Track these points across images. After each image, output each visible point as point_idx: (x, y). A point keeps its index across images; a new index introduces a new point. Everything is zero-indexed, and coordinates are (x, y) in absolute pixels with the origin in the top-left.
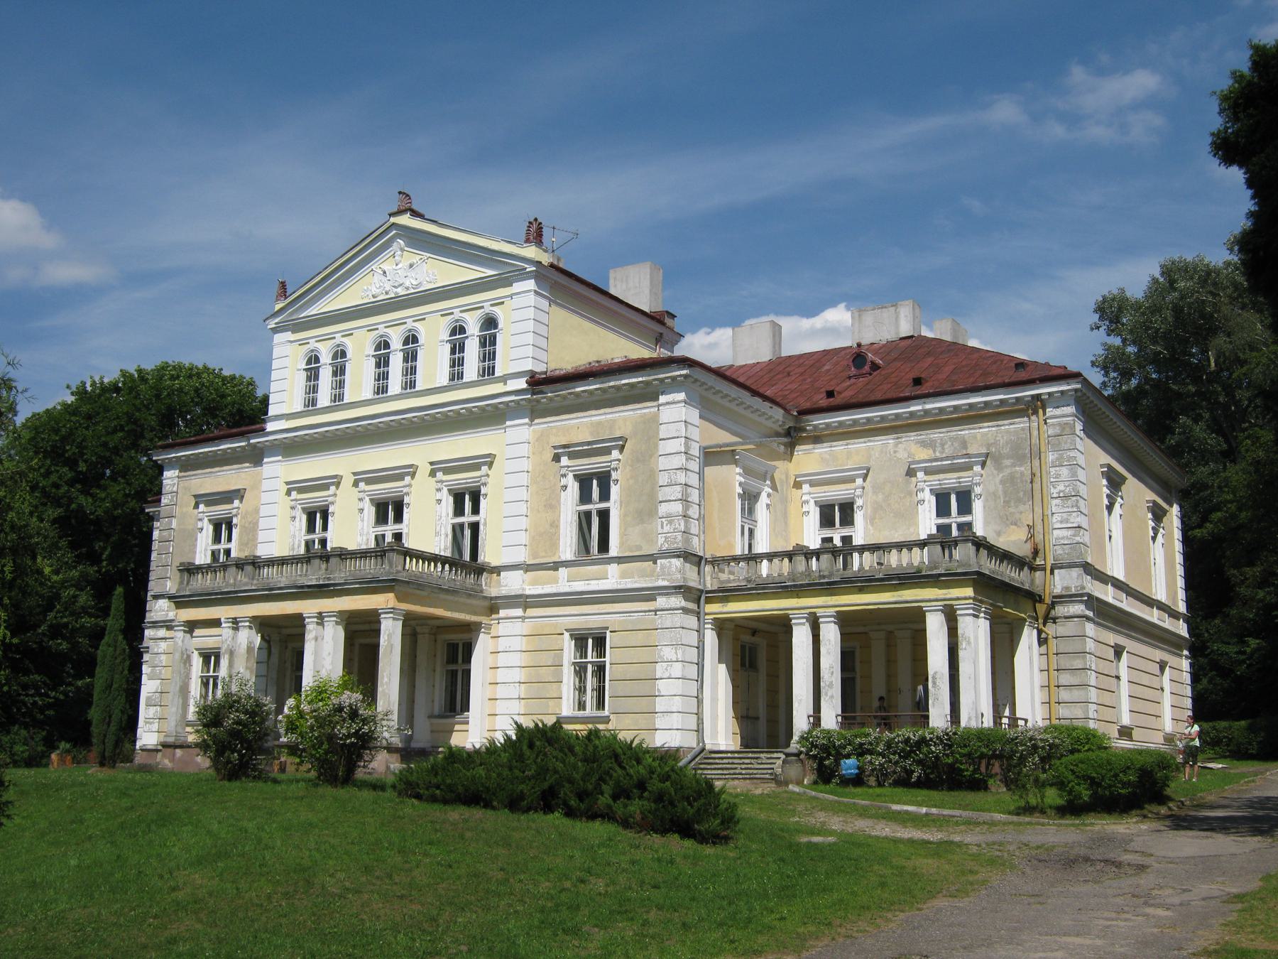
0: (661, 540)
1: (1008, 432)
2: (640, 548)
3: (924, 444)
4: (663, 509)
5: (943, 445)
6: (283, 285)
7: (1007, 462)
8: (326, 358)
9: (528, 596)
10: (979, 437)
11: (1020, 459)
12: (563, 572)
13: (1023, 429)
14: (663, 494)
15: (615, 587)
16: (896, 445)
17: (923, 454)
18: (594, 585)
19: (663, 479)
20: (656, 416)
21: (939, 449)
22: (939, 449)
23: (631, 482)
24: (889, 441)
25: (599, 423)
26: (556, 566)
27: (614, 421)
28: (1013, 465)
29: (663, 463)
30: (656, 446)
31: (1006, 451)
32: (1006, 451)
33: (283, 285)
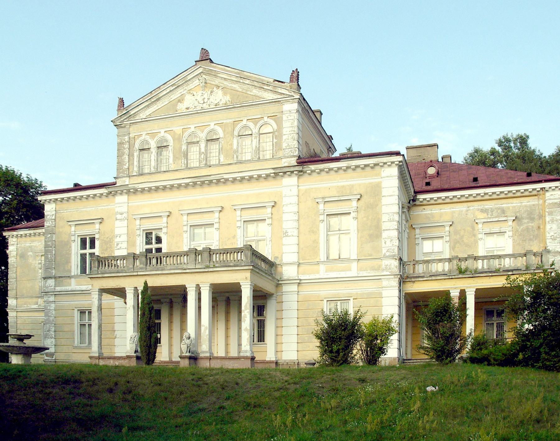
0: (384, 251)
1: (526, 206)
2: (371, 255)
3: (482, 211)
4: (385, 235)
5: (492, 212)
6: (122, 101)
7: (526, 221)
9: (301, 280)
10: (511, 208)
11: (532, 219)
12: (322, 267)
13: (534, 205)
14: (384, 226)
15: (356, 275)
16: (467, 211)
17: (482, 216)
18: (342, 274)
19: (385, 218)
20: (380, 183)
21: (490, 213)
22: (490, 213)
23: (365, 219)
24: (462, 207)
25: (343, 186)
26: (318, 263)
27: (353, 186)
28: (528, 223)
29: (384, 209)
30: (380, 200)
31: (525, 215)
32: (525, 215)
33: (122, 101)
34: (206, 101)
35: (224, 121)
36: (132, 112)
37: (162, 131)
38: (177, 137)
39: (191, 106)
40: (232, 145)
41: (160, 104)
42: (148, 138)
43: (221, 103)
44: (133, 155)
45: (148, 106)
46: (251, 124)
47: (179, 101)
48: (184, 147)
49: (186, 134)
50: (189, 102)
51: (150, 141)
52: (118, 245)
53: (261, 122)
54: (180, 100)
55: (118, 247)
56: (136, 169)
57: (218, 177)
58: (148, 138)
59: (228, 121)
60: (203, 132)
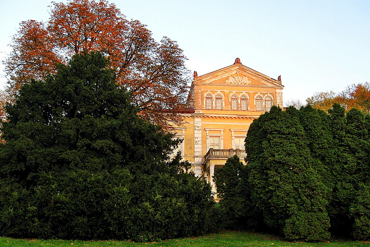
8: (214, 96)
34: (240, 81)
35: (250, 92)
36: (203, 80)
37: (219, 91)
38: (226, 95)
39: (233, 82)
40: (254, 103)
41: (217, 79)
42: (211, 93)
43: (247, 83)
44: (203, 100)
45: (211, 78)
46: (262, 96)
47: (226, 79)
48: (230, 100)
49: (231, 94)
50: (231, 80)
51: (212, 94)
52: (196, 142)
53: (266, 95)
54: (227, 78)
55: (197, 143)
56: (205, 106)
57: (250, 116)
58: (211, 93)
59: (251, 92)
60: (239, 95)
